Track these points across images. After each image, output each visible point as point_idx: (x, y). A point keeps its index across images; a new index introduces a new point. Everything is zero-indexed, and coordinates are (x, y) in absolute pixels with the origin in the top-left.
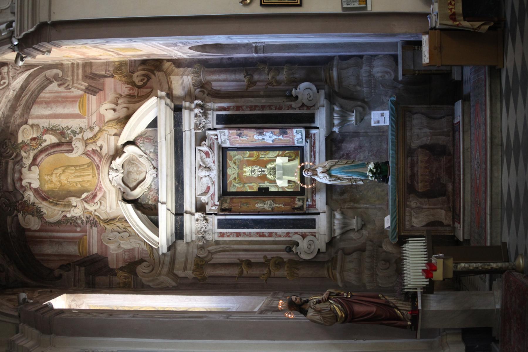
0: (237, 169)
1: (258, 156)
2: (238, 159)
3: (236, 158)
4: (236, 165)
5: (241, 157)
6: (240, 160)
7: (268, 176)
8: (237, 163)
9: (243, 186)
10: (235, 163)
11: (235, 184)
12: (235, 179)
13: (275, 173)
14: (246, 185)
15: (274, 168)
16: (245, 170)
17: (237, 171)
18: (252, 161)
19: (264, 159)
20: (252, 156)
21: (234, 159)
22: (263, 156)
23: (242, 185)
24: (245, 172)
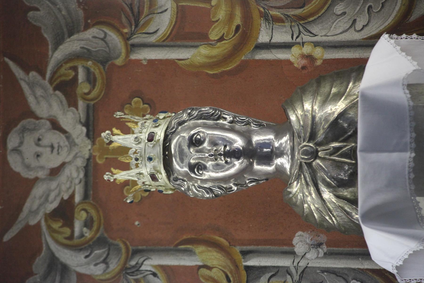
0: (79, 132)
1: (245, 34)
2: (84, 55)
3: (72, 45)
4: (72, 102)
5: (114, 37)
6: (105, 60)
7: (295, 188)
8: (83, 87)
9: (125, 270)
10: (66, 88)
11: (67, 257)
12: (64, 212)
13: (354, 175)
14: (150, 263)
15: (342, 129)
16: (120, 139)
17: (85, 147)
18: (194, 72)
19: (292, 55)
20: (202, 37)
21: (58, 55)
22: (281, 36)
23: (115, 265)
24: (119, 158)
